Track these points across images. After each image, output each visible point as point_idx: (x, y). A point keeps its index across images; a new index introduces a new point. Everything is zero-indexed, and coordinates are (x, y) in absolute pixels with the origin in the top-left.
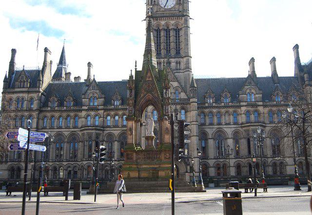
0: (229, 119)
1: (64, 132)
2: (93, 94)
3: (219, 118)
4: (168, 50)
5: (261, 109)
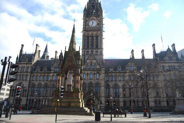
0: (121, 79)
3: (116, 78)
4: (92, 46)
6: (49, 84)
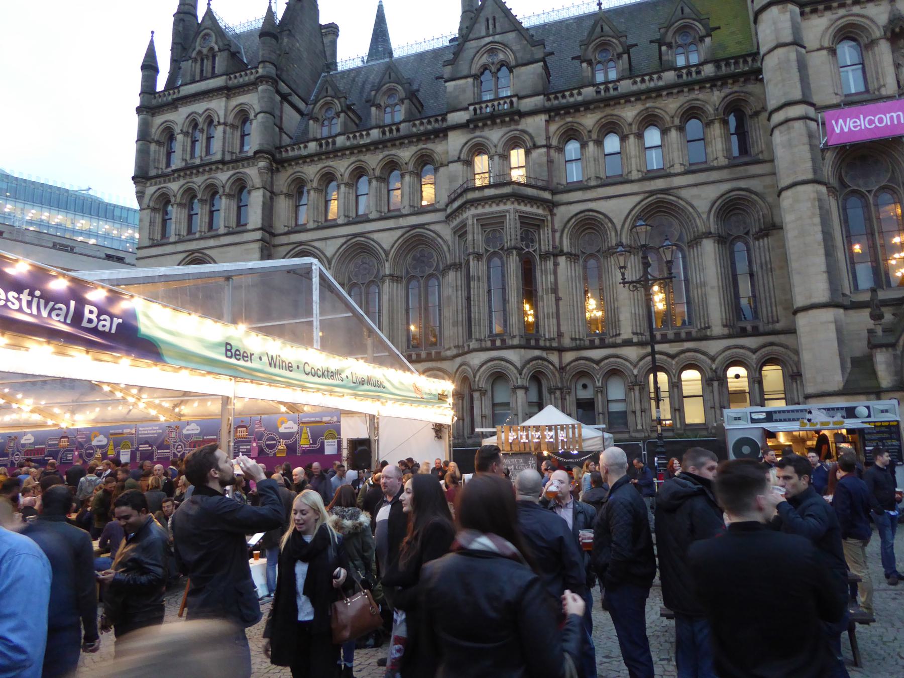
1: (375, 236)
2: (492, 51)
6: (446, 231)
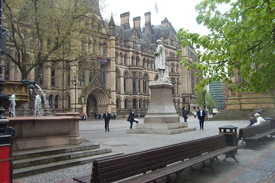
5: (140, 55)
